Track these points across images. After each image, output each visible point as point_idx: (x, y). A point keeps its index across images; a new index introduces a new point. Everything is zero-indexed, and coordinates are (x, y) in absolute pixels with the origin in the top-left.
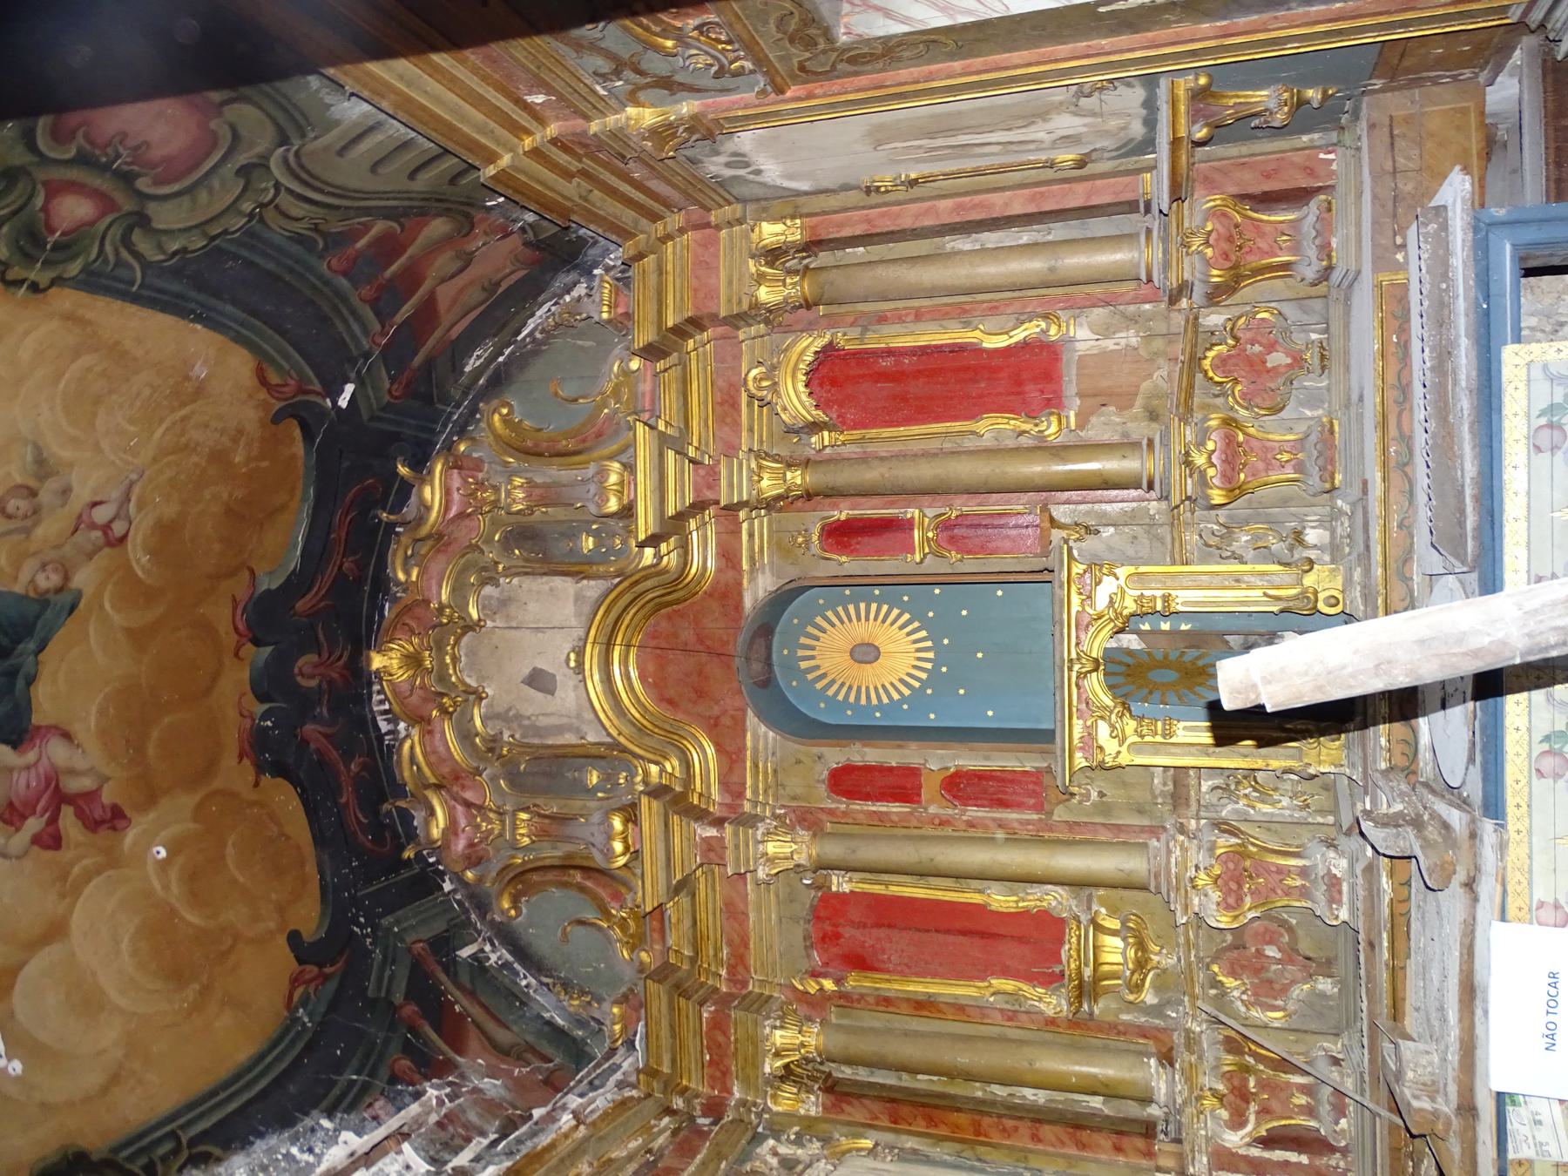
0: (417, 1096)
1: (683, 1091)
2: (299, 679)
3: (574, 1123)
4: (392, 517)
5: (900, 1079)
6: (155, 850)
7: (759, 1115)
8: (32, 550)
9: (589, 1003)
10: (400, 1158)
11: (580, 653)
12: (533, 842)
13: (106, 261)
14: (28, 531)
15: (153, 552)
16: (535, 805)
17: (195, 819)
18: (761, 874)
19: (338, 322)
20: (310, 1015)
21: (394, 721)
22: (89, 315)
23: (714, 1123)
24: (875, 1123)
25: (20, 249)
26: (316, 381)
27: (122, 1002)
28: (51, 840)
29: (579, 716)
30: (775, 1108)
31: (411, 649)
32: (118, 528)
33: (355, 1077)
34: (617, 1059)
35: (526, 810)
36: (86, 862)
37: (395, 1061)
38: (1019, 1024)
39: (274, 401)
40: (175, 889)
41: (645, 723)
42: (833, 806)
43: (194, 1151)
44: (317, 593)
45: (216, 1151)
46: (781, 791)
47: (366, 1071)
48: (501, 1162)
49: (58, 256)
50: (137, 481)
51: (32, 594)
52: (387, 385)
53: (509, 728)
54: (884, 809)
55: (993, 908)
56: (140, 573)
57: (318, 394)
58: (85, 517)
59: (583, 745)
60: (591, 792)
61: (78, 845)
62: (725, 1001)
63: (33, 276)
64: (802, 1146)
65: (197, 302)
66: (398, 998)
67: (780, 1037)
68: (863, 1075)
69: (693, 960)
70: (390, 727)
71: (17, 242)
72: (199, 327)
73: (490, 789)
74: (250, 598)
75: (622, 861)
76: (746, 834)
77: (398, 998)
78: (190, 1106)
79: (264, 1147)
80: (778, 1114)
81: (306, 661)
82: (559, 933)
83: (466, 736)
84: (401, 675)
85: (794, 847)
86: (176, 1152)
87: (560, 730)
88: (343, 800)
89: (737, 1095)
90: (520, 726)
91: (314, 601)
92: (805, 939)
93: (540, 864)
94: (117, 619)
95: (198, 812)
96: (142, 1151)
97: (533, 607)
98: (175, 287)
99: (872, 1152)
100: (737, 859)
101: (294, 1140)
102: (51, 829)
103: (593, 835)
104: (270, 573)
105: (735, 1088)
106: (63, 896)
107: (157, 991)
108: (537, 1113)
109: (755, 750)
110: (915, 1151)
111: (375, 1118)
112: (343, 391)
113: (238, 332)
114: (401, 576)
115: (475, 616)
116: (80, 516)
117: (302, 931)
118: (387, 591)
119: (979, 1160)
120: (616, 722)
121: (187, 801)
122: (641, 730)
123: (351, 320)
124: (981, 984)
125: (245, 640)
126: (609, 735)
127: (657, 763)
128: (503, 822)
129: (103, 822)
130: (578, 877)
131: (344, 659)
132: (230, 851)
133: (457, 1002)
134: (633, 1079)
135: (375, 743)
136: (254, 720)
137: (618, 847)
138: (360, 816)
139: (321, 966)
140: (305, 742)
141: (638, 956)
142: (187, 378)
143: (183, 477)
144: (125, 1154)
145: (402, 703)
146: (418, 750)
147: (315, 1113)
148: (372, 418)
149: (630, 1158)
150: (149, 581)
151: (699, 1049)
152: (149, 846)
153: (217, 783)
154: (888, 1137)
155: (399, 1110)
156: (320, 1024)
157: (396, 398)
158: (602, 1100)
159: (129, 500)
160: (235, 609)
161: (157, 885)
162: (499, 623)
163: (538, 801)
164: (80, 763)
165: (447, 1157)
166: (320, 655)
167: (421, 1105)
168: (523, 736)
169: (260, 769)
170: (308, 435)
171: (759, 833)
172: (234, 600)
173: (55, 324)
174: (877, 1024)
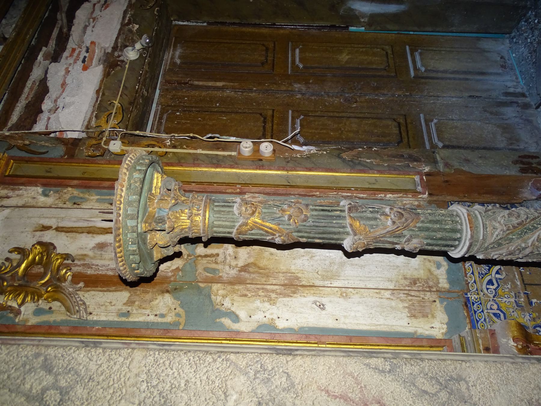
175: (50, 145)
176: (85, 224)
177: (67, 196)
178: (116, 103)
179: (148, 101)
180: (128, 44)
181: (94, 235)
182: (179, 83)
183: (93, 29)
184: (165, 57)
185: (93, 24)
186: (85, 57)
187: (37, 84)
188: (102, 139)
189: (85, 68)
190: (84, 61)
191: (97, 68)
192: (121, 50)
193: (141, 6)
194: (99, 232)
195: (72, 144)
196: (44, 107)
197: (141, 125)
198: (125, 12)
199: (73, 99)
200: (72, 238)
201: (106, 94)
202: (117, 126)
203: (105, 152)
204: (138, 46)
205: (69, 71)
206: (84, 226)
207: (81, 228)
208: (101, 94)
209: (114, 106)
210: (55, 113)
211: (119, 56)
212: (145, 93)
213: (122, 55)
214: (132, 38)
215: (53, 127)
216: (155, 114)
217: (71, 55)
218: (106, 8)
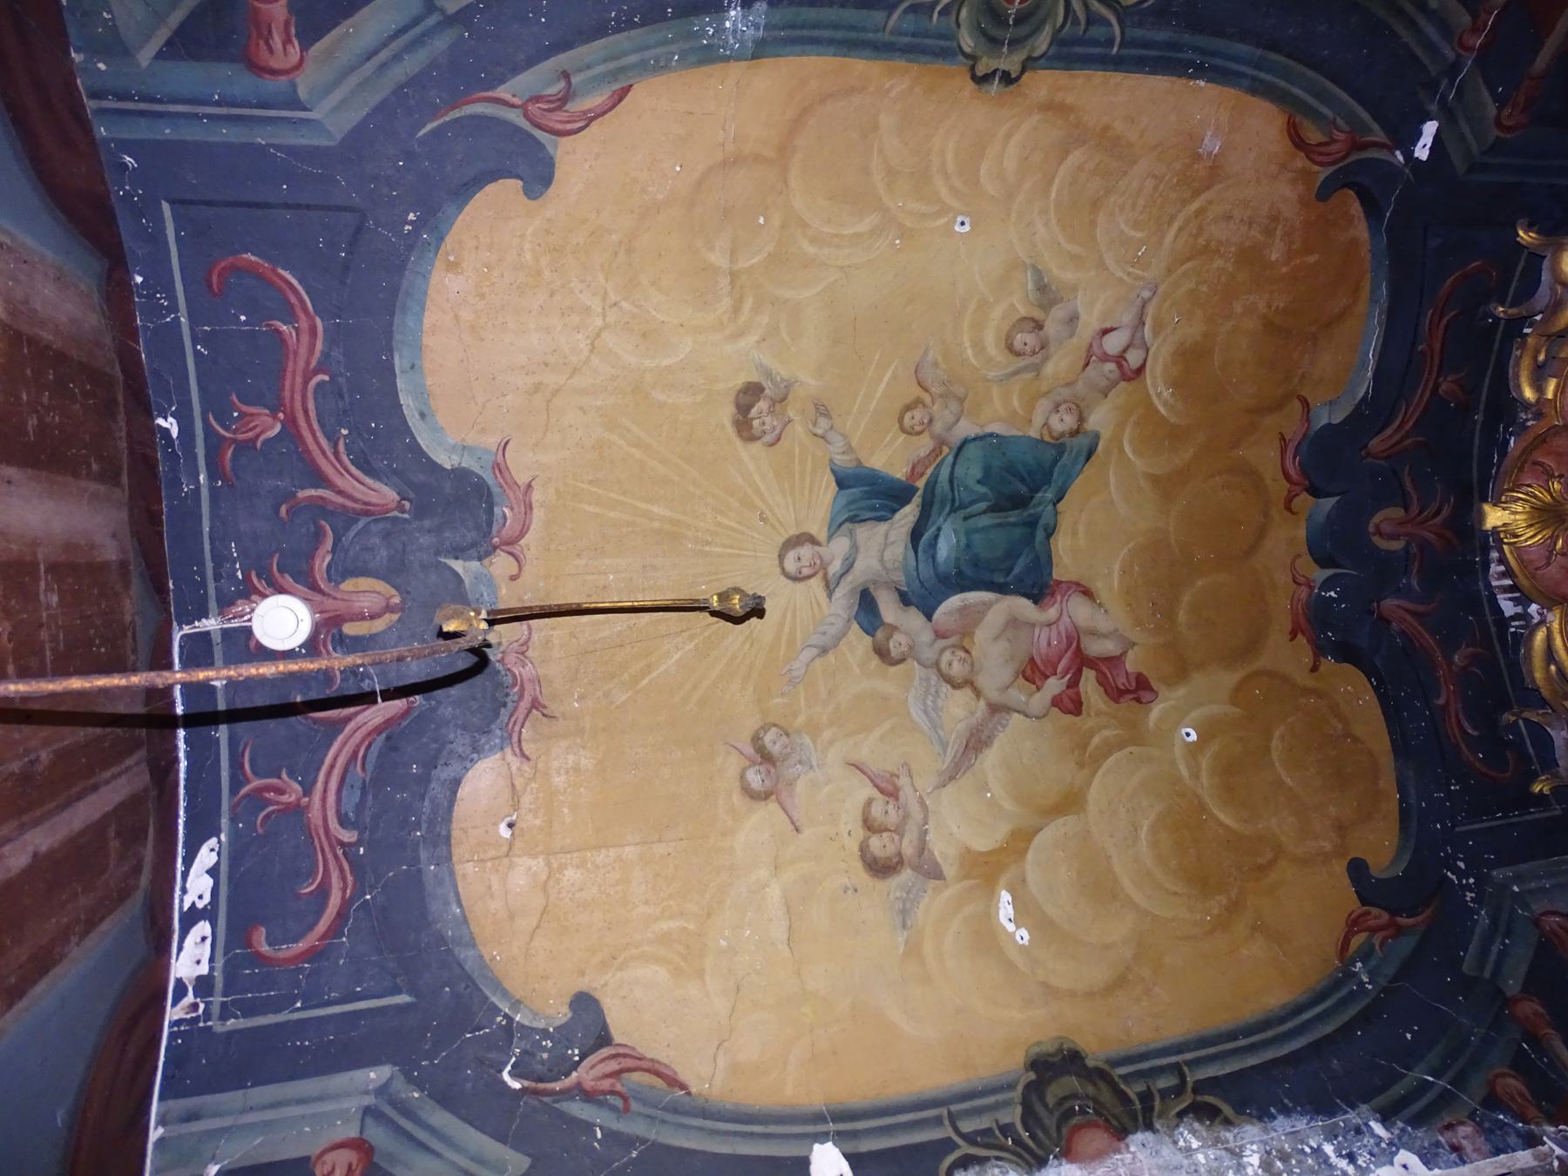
0: (1531, 1141)
2: (1376, 540)
4: (1510, 311)
6: (1184, 731)
8: (1044, 387)
13: (1076, 22)
14: (1037, 369)
15: (1176, 384)
17: (1234, 704)
19: (1401, 30)
20: (1370, 973)
21: (1524, 601)
22: (1070, 100)
25: (984, 33)
26: (1375, 126)
27: (1138, 898)
28: (1071, 704)
32: (1134, 359)
33: (1430, 1079)
36: (1106, 733)
37: (1497, 1076)
39: (1316, 168)
40: (1204, 779)
43: (1199, 1098)
44: (1400, 426)
45: (1227, 1110)
47: (1450, 1074)
49: (1023, 30)
50: (1150, 299)
51: (1047, 438)
52: (1492, 110)
56: (1162, 410)
57: (1381, 146)
58: (1095, 348)
61: (1099, 713)
63: (1003, 64)
65: (1195, 49)
66: (1512, 986)
70: (1519, 609)
71: (979, 25)
72: (1202, 83)
74: (1305, 435)
77: (1512, 986)
78: (1203, 1042)
79: (1289, 1130)
81: (1387, 516)
84: (1530, 538)
86: (1179, 1090)
88: (1441, 701)
91: (1397, 437)
94: (1140, 465)
95: (1238, 694)
96: (1140, 1074)
98: (1162, 35)
101: (1331, 1136)
102: (1071, 692)
104: (1331, 402)
106: (1081, 765)
107: (1175, 893)
111: (1456, 1148)
112: (1420, 134)
113: (1254, 79)
114: (1529, 394)
116: (1091, 346)
117: (1371, 861)
118: (1512, 420)
121: (1229, 679)
123: (1421, 20)
125: (1298, 489)
129: (1128, 691)
131: (1445, 512)
132: (1275, 744)
135: (1493, 629)
136: (1311, 588)
138: (1466, 725)
139: (1394, 913)
140: (1384, 621)
142: (1197, 157)
143: (1204, 288)
145: (1532, 576)
146: (1558, 641)
147: (1364, 1108)
148: (1470, 170)
150: (1173, 420)
152: (1177, 725)
153: (1263, 662)
155: (1497, 1152)
156: (1384, 990)
157: (1509, 129)
159: (1144, 324)
160: (1283, 452)
161: (1184, 771)
164: (1103, 624)
166: (1406, 510)
167: (1536, 1157)
169: (1320, 650)
170: (1372, 209)
172: (1283, 438)
173: (1036, 117)
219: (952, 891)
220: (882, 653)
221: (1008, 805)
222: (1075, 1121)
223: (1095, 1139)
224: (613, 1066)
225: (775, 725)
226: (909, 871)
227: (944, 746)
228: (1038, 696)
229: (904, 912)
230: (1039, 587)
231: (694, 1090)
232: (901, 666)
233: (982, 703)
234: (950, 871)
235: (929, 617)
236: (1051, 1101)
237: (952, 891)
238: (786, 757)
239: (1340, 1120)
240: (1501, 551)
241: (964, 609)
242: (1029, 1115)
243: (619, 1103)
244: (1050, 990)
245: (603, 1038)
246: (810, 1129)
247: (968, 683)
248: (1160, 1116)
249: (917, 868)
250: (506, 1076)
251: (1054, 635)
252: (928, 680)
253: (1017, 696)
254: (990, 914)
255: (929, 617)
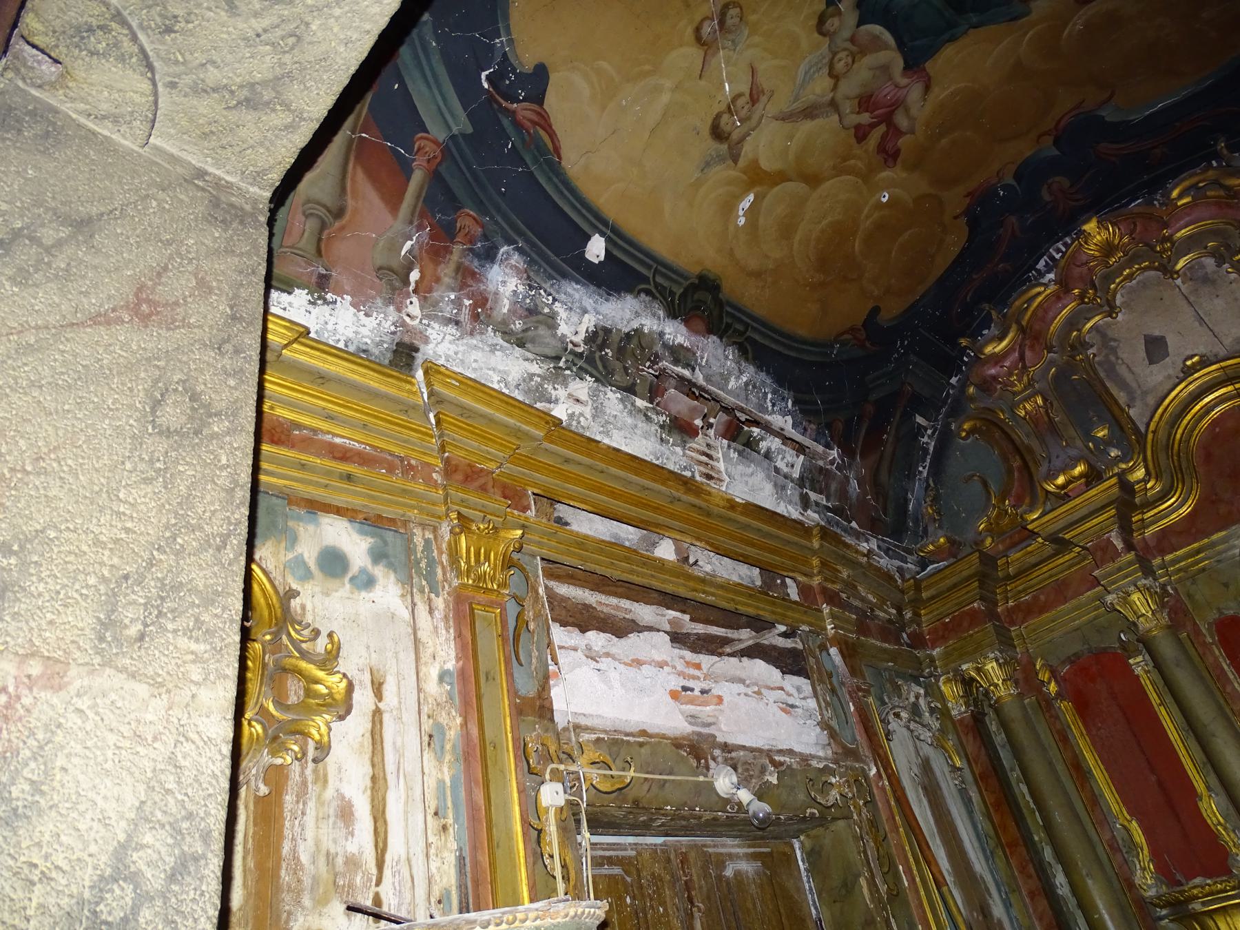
0: (828, 446)
1: (917, 614)
2: (1046, 186)
3: (866, 552)
5: (1012, 770)
7: (931, 675)
9: (935, 520)
10: (795, 458)
11: (1204, 363)
12: (1024, 418)
16: (1051, 403)
18: (1110, 598)
23: (908, 645)
24: (974, 765)
27: (796, 246)
28: (861, 134)
29: (1145, 393)
30: (941, 684)
31: (1116, 242)
34: (910, 558)
35: (1045, 400)
36: (860, 164)
38: (1111, 856)
41: (1176, 446)
42: (1204, 631)
45: (750, 355)
46: (1188, 583)
48: (822, 520)
53: (1099, 349)
54: (1232, 677)
55: (1200, 804)
59: (1122, 410)
60: (1088, 436)
62: (992, 615)
64: (931, 715)
66: (873, 397)
67: (991, 666)
68: (999, 739)
69: (1008, 578)
73: (1044, 364)
75: (1051, 488)
76: (1135, 571)
77: (873, 397)
78: (764, 324)
80: (939, 688)
81: (1062, 181)
82: (969, 473)
83: (1073, 322)
84: (1092, 249)
85: (1149, 614)
86: (742, 334)
87: (1124, 385)
88: (975, 276)
89: (934, 653)
90: (1107, 356)
92: (1074, 654)
93: (1009, 431)
96: (733, 316)
97: (1219, 303)
99: (954, 769)
100: (1110, 575)
101: (774, 393)
103: (1058, 457)
105: (938, 649)
106: (834, 168)
108: (854, 524)
109: (1213, 545)
110: (970, 799)
111: (805, 429)
115: (1179, 267)
119: (992, 853)
120: (1162, 424)
122: (1168, 446)
124: (1125, 813)
126: (1148, 425)
127: (1148, 473)
128: (1025, 389)
129: (887, 153)
130: (1017, 463)
132: (906, 235)
133: (888, 434)
134: (908, 576)
136: (999, 182)
137: (1061, 480)
138: (970, 294)
141: (986, 537)
144: (729, 309)
146: (1040, 299)
147: (792, 393)
149: (863, 600)
151: (950, 611)
152: (886, 188)
154: (967, 773)
155: (815, 440)
158: (884, 562)
161: (866, 211)
162: (1183, 288)
163: (1055, 404)
164: (914, 111)
165: (807, 485)
168: (1100, 363)
169: (968, 212)
171: (1144, 581)
174: (1042, 736)
175: (533, 667)
176: (390, 767)
177: (443, 719)
178: (632, 773)
179: (644, 829)
180: (740, 770)
181: (369, 792)
182: (688, 886)
183: (742, 695)
184: (729, 841)
185: (750, 693)
186: (692, 690)
187: (627, 616)
188: (561, 762)
189: (674, 695)
190: (685, 689)
191: (681, 717)
192: (726, 760)
193: (811, 780)
194: (376, 802)
195: (542, 707)
196: (592, 634)
197: (597, 825)
198: (790, 752)
199: (617, 685)
200: (362, 745)
201: (643, 750)
202: (588, 783)
203: (537, 774)
204: (744, 796)
205: (662, 668)
206: (386, 767)
207: (383, 760)
208: (641, 740)
209: (624, 770)
210: (587, 657)
211: (714, 759)
212: (659, 823)
213: (717, 763)
214: (751, 776)
215: (562, 657)
216: (614, 844)
217: (688, 664)
218: (783, 710)
219: (733, 173)
220: (822, 20)
221: (791, 157)
222: (699, 312)
223: (701, 326)
224: (535, 118)
225: (741, 9)
226: (726, 146)
227: (796, 99)
228: (854, 116)
229: (708, 164)
230: (914, 62)
231: (563, 163)
232: (821, 38)
233: (831, 95)
234: (742, 162)
235: (858, 25)
236: (696, 297)
237: (733, 173)
238: (730, 32)
239: (781, 390)
240: (1072, 243)
241: (876, 38)
242: (684, 296)
243: (527, 138)
244: (731, 253)
245: (538, 97)
246: (601, 226)
247: (835, 76)
248: (727, 337)
249: (729, 147)
250: (484, 75)
251: (892, 94)
252: (824, 58)
253: (847, 107)
254: (739, 198)
255: (858, 25)
